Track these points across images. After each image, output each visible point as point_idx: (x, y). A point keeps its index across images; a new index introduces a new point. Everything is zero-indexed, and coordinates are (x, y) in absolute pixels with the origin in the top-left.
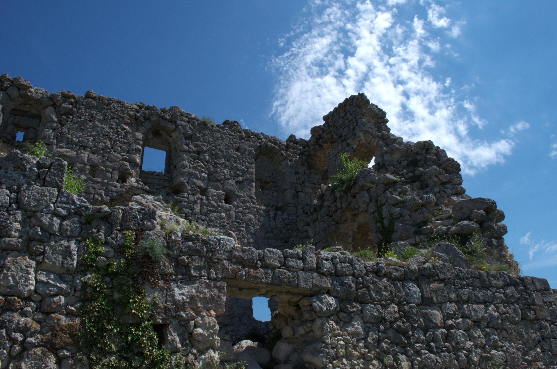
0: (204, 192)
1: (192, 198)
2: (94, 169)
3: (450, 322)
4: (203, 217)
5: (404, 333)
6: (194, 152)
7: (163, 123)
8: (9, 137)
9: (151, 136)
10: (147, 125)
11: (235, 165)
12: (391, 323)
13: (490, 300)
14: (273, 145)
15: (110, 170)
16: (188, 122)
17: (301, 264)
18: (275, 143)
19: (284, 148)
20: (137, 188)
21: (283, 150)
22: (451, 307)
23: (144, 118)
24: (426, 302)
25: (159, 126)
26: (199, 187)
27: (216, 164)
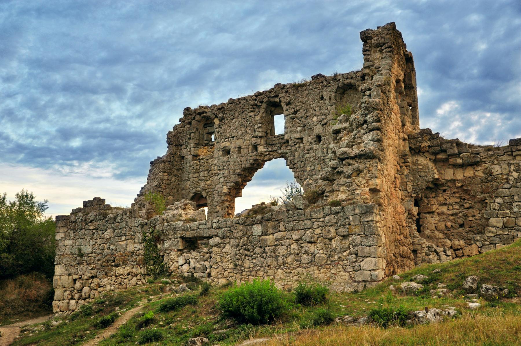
0: (301, 139)
1: (293, 149)
2: (240, 148)
3: (276, 243)
4: (301, 159)
5: (249, 250)
6: (293, 114)
7: (272, 100)
8: (206, 142)
9: (273, 109)
10: (264, 106)
11: (320, 112)
12: (242, 246)
13: (309, 227)
14: (349, 81)
15: (247, 146)
16: (286, 92)
17: (204, 226)
18: (352, 78)
19: (360, 78)
20: (265, 152)
21: (358, 81)
22: (278, 235)
23: (260, 102)
24: (265, 233)
25: (270, 103)
26: (298, 139)
27: (307, 117)
